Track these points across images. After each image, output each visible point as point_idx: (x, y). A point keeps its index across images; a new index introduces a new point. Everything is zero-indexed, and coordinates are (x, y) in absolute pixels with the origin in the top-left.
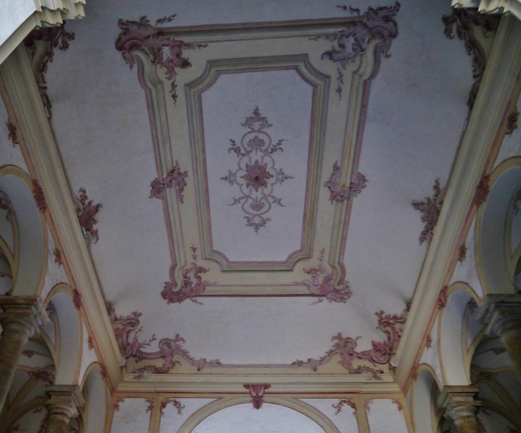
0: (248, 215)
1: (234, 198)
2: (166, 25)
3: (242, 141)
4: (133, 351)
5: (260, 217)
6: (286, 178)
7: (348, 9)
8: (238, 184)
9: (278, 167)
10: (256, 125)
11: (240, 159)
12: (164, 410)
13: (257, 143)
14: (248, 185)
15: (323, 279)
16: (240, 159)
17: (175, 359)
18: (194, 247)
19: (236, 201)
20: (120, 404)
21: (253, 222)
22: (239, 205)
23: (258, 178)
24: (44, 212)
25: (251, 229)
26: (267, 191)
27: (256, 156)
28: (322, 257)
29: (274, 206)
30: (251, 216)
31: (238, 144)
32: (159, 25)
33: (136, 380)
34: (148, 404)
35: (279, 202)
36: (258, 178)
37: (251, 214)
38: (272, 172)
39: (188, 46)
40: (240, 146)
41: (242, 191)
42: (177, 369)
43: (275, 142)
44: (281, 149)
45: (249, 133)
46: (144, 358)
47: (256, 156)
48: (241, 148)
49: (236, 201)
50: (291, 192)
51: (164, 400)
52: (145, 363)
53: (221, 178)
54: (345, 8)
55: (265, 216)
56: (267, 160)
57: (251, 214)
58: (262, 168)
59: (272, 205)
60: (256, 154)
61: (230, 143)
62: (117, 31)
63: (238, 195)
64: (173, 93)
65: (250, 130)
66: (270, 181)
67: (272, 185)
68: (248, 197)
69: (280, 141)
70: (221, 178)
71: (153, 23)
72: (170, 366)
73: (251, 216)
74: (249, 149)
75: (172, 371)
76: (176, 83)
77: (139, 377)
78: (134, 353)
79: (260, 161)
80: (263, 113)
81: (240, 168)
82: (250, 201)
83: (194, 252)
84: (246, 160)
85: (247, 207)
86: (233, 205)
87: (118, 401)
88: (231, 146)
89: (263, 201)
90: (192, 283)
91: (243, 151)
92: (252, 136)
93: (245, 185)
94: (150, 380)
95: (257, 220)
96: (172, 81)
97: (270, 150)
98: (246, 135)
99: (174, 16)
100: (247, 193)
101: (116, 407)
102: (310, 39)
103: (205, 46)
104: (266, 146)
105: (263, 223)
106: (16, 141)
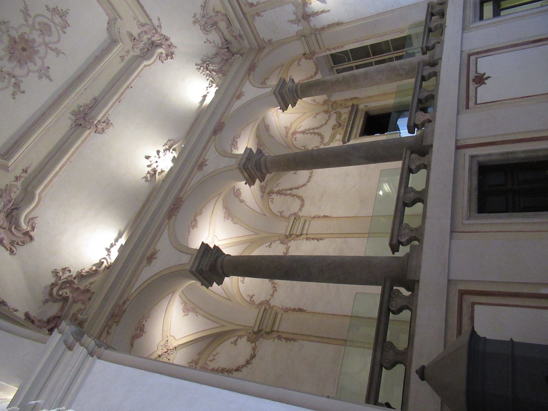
0: (60, 32)
3: (6, 88)
4: (225, 52)
8: (43, 62)
12: (255, 3)
14: (37, 52)
17: (212, 14)
18: (120, 60)
19: (58, 52)
20: (266, 40)
21: (62, 22)
22: (59, 46)
24: (182, 198)
26: (26, 30)
30: (59, 28)
33: (244, 37)
34: (256, 18)
37: (58, 31)
42: (219, 8)
46: (226, 40)
49: (58, 52)
51: (247, 6)
52: (228, 36)
53: (51, 80)
55: (49, 15)
57: (58, 31)
60: (4, 66)
61: (16, 97)
62: (20, 250)
63: (51, 54)
64: (23, 175)
68: (46, 45)
70: (51, 80)
72: (220, 15)
73: (59, 28)
74: (7, 76)
75: (223, 11)
76: (14, 179)
77: (240, 36)
78: (226, 50)
79: (6, 59)
82: (47, 39)
83: (124, 56)
84: (18, 72)
85: (54, 38)
86: (63, 53)
87: (265, 42)
88: (18, 93)
89: (37, 27)
90: (149, 39)
94: (238, 26)
95: (57, 19)
96: (15, 183)
100: (43, 47)
101: (270, 41)
105: (55, 10)
106: (154, 251)
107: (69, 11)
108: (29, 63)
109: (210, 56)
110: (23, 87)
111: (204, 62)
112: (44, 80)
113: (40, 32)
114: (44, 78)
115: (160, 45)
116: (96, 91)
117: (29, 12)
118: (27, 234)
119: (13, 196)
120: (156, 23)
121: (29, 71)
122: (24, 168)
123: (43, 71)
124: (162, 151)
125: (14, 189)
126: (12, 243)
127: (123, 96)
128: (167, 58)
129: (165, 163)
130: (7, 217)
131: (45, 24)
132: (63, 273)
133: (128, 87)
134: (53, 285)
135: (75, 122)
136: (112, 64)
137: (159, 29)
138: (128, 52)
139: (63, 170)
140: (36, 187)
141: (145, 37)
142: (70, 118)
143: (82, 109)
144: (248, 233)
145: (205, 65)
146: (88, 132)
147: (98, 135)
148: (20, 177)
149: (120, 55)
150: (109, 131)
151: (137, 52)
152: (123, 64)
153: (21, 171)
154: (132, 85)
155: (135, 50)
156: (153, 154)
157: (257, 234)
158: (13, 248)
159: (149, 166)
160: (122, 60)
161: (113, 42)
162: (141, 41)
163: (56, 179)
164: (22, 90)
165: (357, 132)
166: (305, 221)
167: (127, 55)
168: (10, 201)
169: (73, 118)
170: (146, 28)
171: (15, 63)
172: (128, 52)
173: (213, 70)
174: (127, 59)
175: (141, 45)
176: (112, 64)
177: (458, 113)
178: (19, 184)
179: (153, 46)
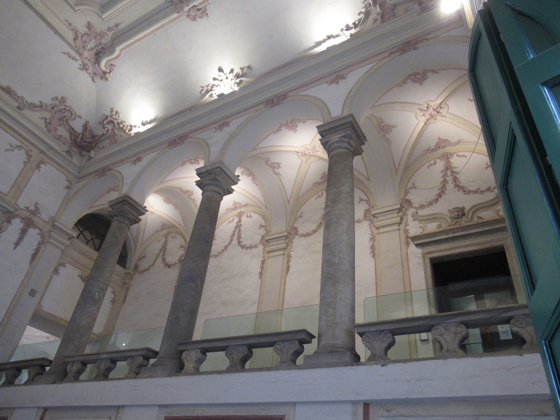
2: (73, 53)
32: (77, 57)
64: (114, 28)
71: (80, 62)
76: (107, 29)
99: (65, 53)
103: (67, 21)
118: (105, 73)
119: (103, 41)
125: (106, 37)
129: (227, 86)
130: (96, 54)
132: (116, 115)
134: (107, 117)
144: (261, 199)
146: (176, 15)
148: (112, 29)
150: (202, 22)
153: (114, 25)
156: (227, 70)
157: (266, 207)
158: (95, 78)
159: (214, 79)
163: (137, 44)
165: (441, 251)
166: (268, 252)
168: (100, 44)
177: (160, 406)
178: (110, 34)
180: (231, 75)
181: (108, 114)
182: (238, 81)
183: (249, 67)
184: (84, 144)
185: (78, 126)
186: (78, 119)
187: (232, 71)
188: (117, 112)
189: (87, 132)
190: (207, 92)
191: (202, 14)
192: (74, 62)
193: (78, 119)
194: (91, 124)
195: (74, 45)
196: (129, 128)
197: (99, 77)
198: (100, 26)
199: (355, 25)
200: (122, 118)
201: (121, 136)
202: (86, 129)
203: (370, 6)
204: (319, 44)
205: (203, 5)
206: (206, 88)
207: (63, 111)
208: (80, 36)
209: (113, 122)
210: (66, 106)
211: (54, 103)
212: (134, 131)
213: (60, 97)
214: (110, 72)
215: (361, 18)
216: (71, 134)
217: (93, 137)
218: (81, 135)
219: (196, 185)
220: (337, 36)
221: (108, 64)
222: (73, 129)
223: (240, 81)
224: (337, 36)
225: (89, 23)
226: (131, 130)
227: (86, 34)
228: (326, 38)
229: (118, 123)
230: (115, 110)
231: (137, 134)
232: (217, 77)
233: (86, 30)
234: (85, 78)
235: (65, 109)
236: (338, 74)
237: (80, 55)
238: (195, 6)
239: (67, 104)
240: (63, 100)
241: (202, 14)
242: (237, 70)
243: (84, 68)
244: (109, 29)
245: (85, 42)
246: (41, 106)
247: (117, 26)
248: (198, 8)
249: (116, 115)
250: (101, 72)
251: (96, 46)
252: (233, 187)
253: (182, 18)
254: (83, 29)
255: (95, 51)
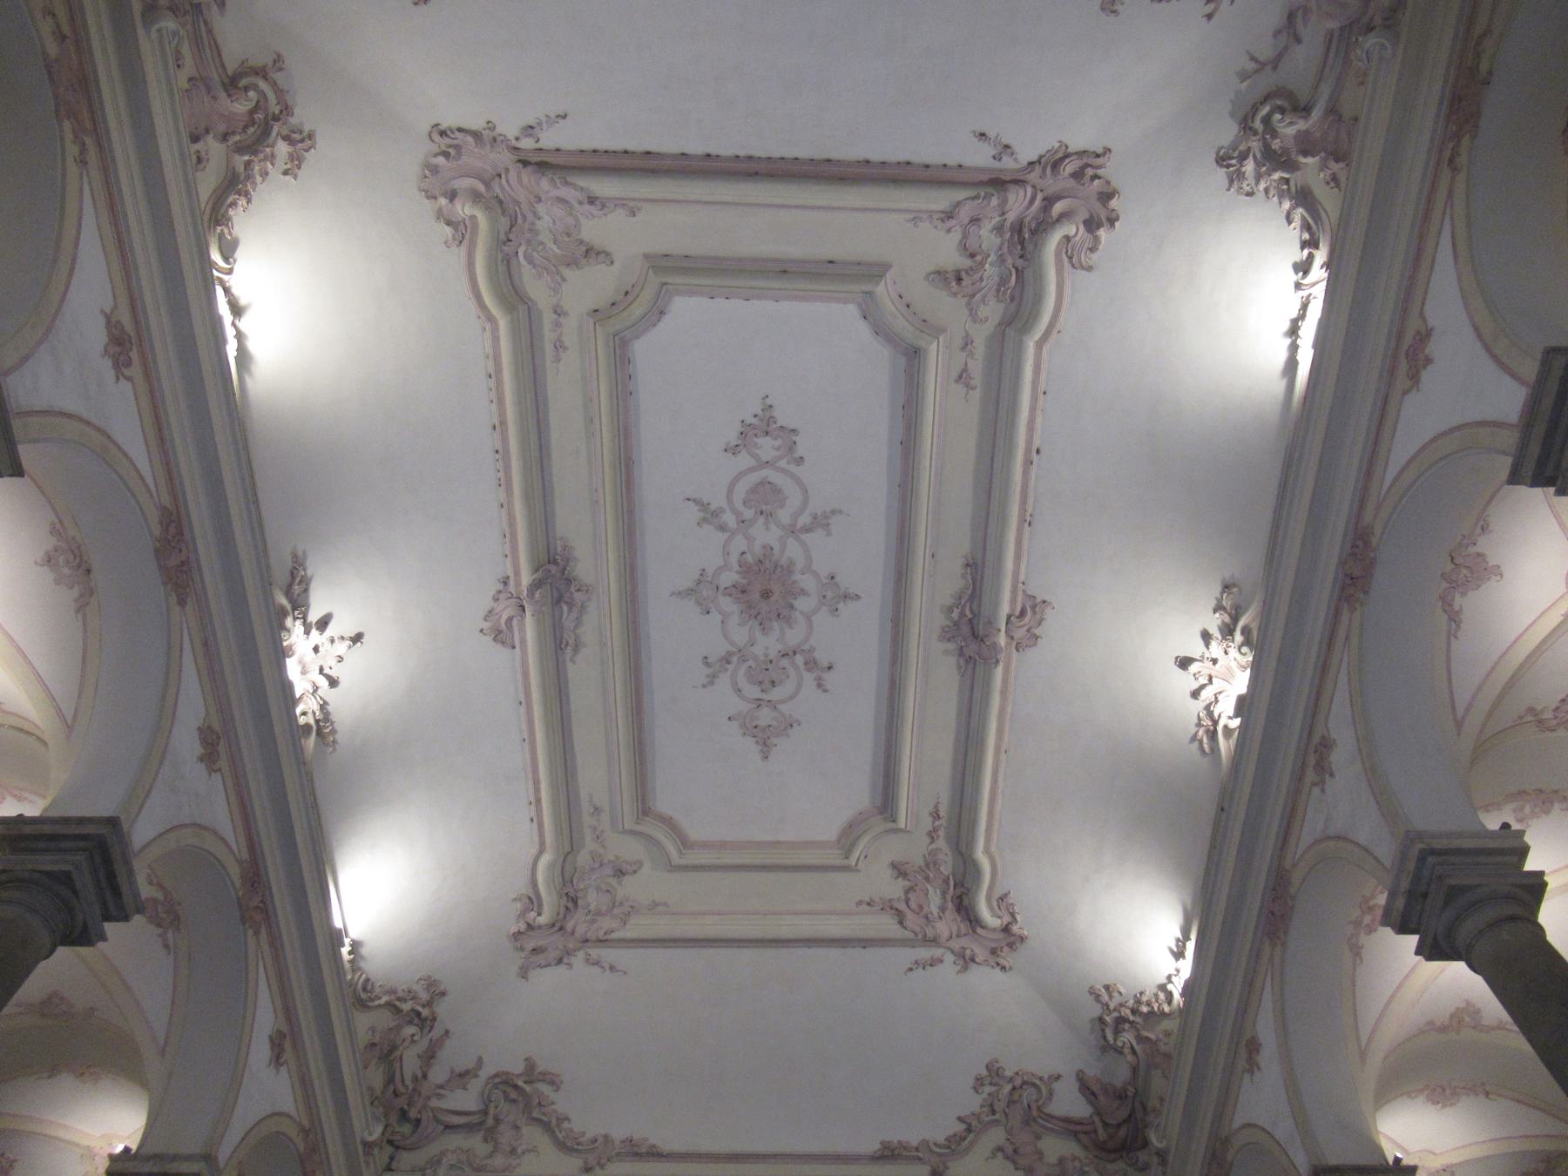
0: (793, 468)
1: (829, 534)
2: (924, 953)
5: (755, 457)
6: (690, 592)
7: (607, 966)
8: (815, 574)
9: (716, 617)
10: (765, 717)
11: (806, 640)
13: (766, 676)
14: (789, 569)
15: (539, 224)
16: (806, 640)
19: (822, 522)
21: (779, 442)
23: (763, 589)
25: (784, 417)
26: (739, 544)
27: (768, 644)
28: (557, 325)
29: (719, 501)
30: (783, 463)
31: (809, 678)
32: (938, 952)
35: (709, 516)
36: (763, 589)
37: (784, 471)
38: (727, 604)
39: (889, 907)
40: (804, 673)
41: (806, 550)
43: (724, 681)
44: (707, 665)
45: (783, 701)
47: (768, 644)
48: (802, 667)
49: (822, 522)
50: (680, 550)
53: (858, 597)
54: (612, 968)
55: (744, 460)
56: (740, 635)
57: (784, 471)
58: (751, 612)
59: (724, 504)
61: (828, 687)
63: (815, 539)
65: (783, 708)
66: (729, 578)
67: (725, 567)
68: (792, 531)
69: (712, 683)
70: (858, 597)
73: (783, 463)
74: (785, 662)
76: (928, 840)
79: (758, 634)
80: (750, 746)
81: (809, 618)
82: (784, 516)
83: (965, 370)
84: (794, 636)
85: (794, 500)
86: (833, 512)
88: (826, 676)
89: (748, 514)
90: (999, 229)
91: (799, 659)
92: (775, 694)
93: (799, 566)
95: (767, 447)
96: (933, 846)
97: (735, 658)
98: (791, 698)
100: (791, 542)
102: (665, 904)
104: (742, 671)
105: (747, 433)
107: (768, 401)
108: (796, 604)
109: (1266, 52)
110: (823, 658)
111: (1246, 125)
112: (846, 609)
113: (761, 520)
114: (841, 606)
115: (1043, 226)
116: (960, 545)
117: (713, 507)
118: (1006, 929)
119: (946, 869)
120: (979, 157)
121: (809, 618)
122: (931, 808)
123: (829, 594)
124: (1215, 632)
125: (941, 857)
126: (993, 952)
127: (1031, 501)
128: (1097, 239)
131: (754, 490)
132: (1111, 997)
133: (1028, 462)
134: (1101, 1020)
135: (961, 654)
136: (950, 415)
137: (1007, 163)
138: (967, 343)
139: (1000, 778)
140: (971, 842)
141: (987, 237)
142: (946, 652)
143: (955, 615)
145: (1255, 145)
146: (999, 672)
147: (1031, 654)
148: (935, 830)
149: (954, 375)
150: (1052, 627)
151: (992, 311)
152: (976, 395)
154: (1036, 443)
155: (983, 311)
156: (1195, 648)
158: (1002, 961)
159: (1195, 694)
160: (969, 387)
161: (913, 356)
162: (982, 264)
163: (998, 807)
164: (826, 664)
167: (971, 355)
168: (946, 881)
169: (951, 646)
170: (965, 213)
171: (776, 625)
172: (967, 343)
173: (1307, 145)
174: (976, 367)
175: (990, 271)
176: (950, 415)
178: (941, 843)
179: (1032, 219)
180: (1214, 644)
181: (1096, 1010)
182: (1239, 638)
183: (1226, 587)
184: (1122, 1133)
185: (1069, 1103)
186: (1056, 1086)
187: (1206, 637)
188: (1107, 987)
189: (1101, 1098)
190: (1212, 735)
191: (1034, 612)
192: (939, 968)
193: (1056, 1086)
194: (1091, 1072)
195: (908, 934)
196: (1162, 996)
197: (1006, 949)
198: (914, 849)
199: (1311, 244)
200: (1127, 990)
201: (1167, 1034)
202: (1093, 1094)
203: (1287, 181)
204: (1291, 365)
205: (1020, 593)
206: (1201, 733)
207: (1016, 1097)
208: (902, 906)
209: (1121, 1020)
210: (1011, 1080)
211: (985, 1096)
212: (1176, 989)
213: (985, 1073)
214: (1012, 915)
215: (1303, 218)
216: (1075, 1134)
217: (1121, 1096)
218: (1096, 1119)
219: (1429, 958)
220: (1304, 306)
221: (995, 904)
222: (1067, 1120)
223: (1243, 633)
224: (1304, 306)
225: (894, 866)
226: (1169, 995)
227: (907, 891)
228: (1288, 341)
229: (1134, 1011)
230: (1099, 987)
231: (1188, 989)
232: (1195, 685)
233: (902, 883)
234: (984, 978)
235: (1014, 1088)
236: (1405, 347)
237: (934, 941)
238: (1009, 617)
239: (1009, 1073)
240: (994, 1072)
241: (1034, 612)
242: (1213, 623)
243: (966, 961)
244: (932, 835)
245: (921, 907)
246: (969, 1130)
247: (936, 815)
248: (1017, 612)
249: (1111, 997)
250: (1001, 936)
251: (944, 893)
252: (1529, 866)
253: (1014, 664)
254: (894, 889)
255: (950, 905)
